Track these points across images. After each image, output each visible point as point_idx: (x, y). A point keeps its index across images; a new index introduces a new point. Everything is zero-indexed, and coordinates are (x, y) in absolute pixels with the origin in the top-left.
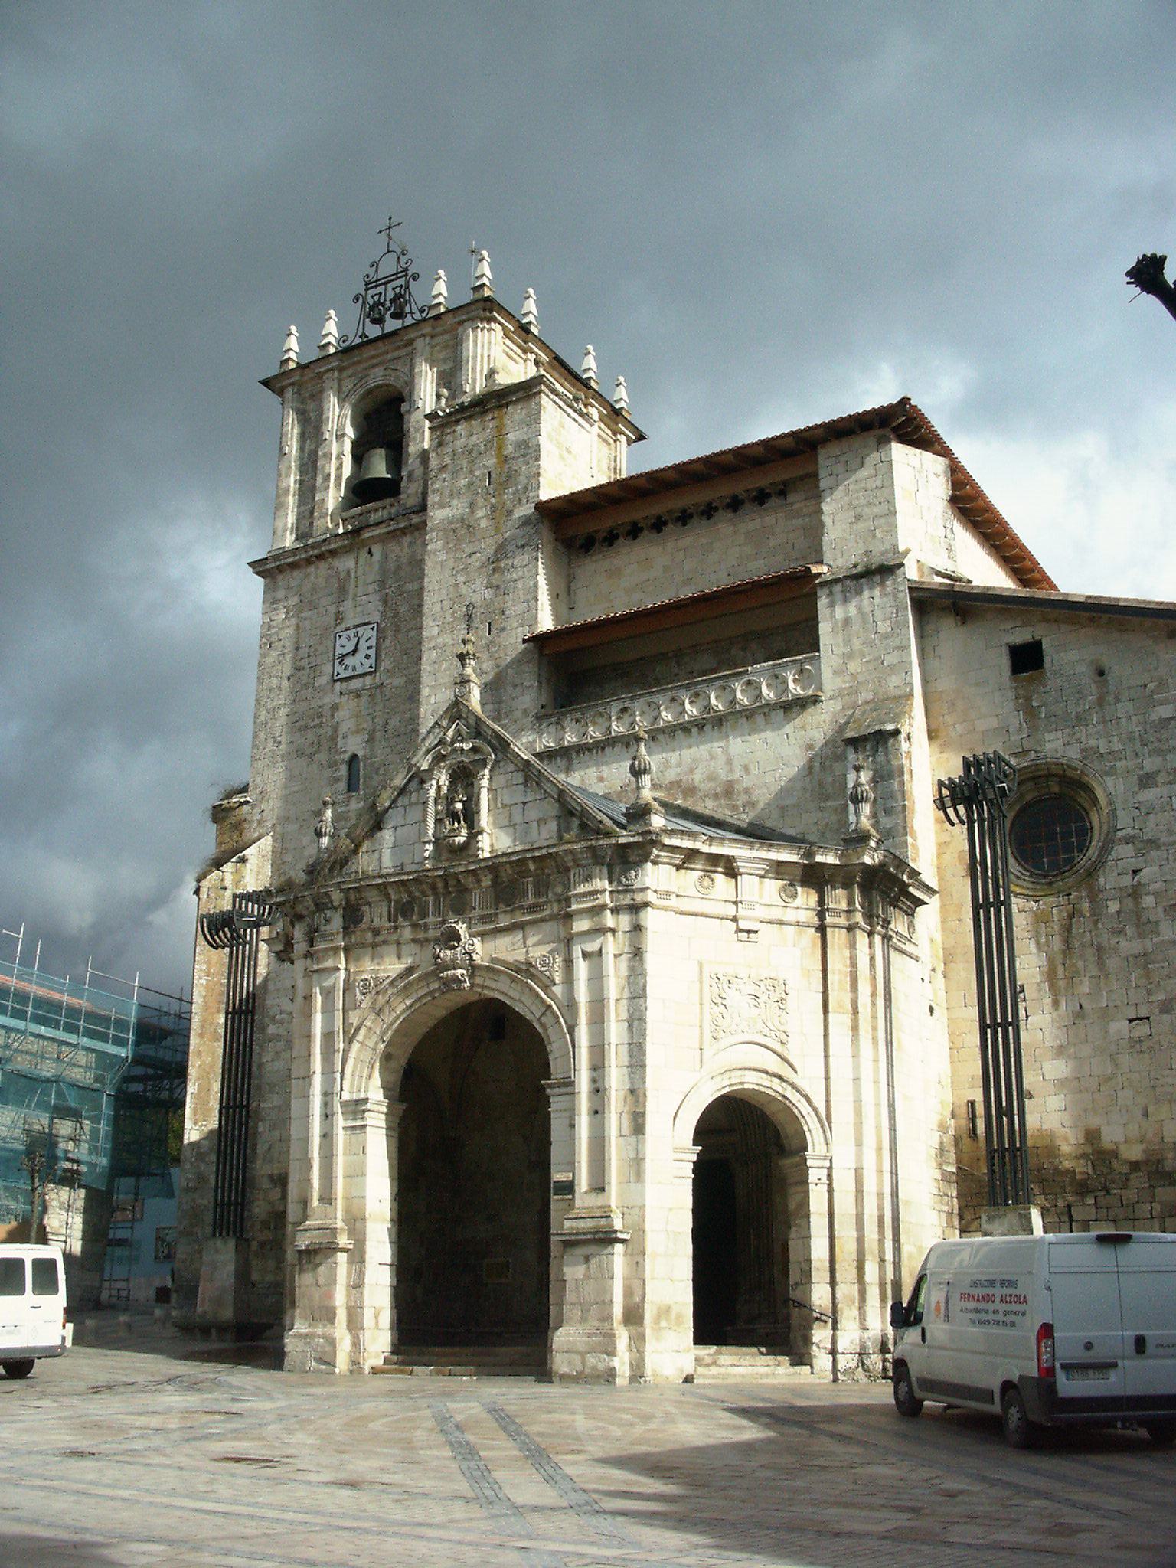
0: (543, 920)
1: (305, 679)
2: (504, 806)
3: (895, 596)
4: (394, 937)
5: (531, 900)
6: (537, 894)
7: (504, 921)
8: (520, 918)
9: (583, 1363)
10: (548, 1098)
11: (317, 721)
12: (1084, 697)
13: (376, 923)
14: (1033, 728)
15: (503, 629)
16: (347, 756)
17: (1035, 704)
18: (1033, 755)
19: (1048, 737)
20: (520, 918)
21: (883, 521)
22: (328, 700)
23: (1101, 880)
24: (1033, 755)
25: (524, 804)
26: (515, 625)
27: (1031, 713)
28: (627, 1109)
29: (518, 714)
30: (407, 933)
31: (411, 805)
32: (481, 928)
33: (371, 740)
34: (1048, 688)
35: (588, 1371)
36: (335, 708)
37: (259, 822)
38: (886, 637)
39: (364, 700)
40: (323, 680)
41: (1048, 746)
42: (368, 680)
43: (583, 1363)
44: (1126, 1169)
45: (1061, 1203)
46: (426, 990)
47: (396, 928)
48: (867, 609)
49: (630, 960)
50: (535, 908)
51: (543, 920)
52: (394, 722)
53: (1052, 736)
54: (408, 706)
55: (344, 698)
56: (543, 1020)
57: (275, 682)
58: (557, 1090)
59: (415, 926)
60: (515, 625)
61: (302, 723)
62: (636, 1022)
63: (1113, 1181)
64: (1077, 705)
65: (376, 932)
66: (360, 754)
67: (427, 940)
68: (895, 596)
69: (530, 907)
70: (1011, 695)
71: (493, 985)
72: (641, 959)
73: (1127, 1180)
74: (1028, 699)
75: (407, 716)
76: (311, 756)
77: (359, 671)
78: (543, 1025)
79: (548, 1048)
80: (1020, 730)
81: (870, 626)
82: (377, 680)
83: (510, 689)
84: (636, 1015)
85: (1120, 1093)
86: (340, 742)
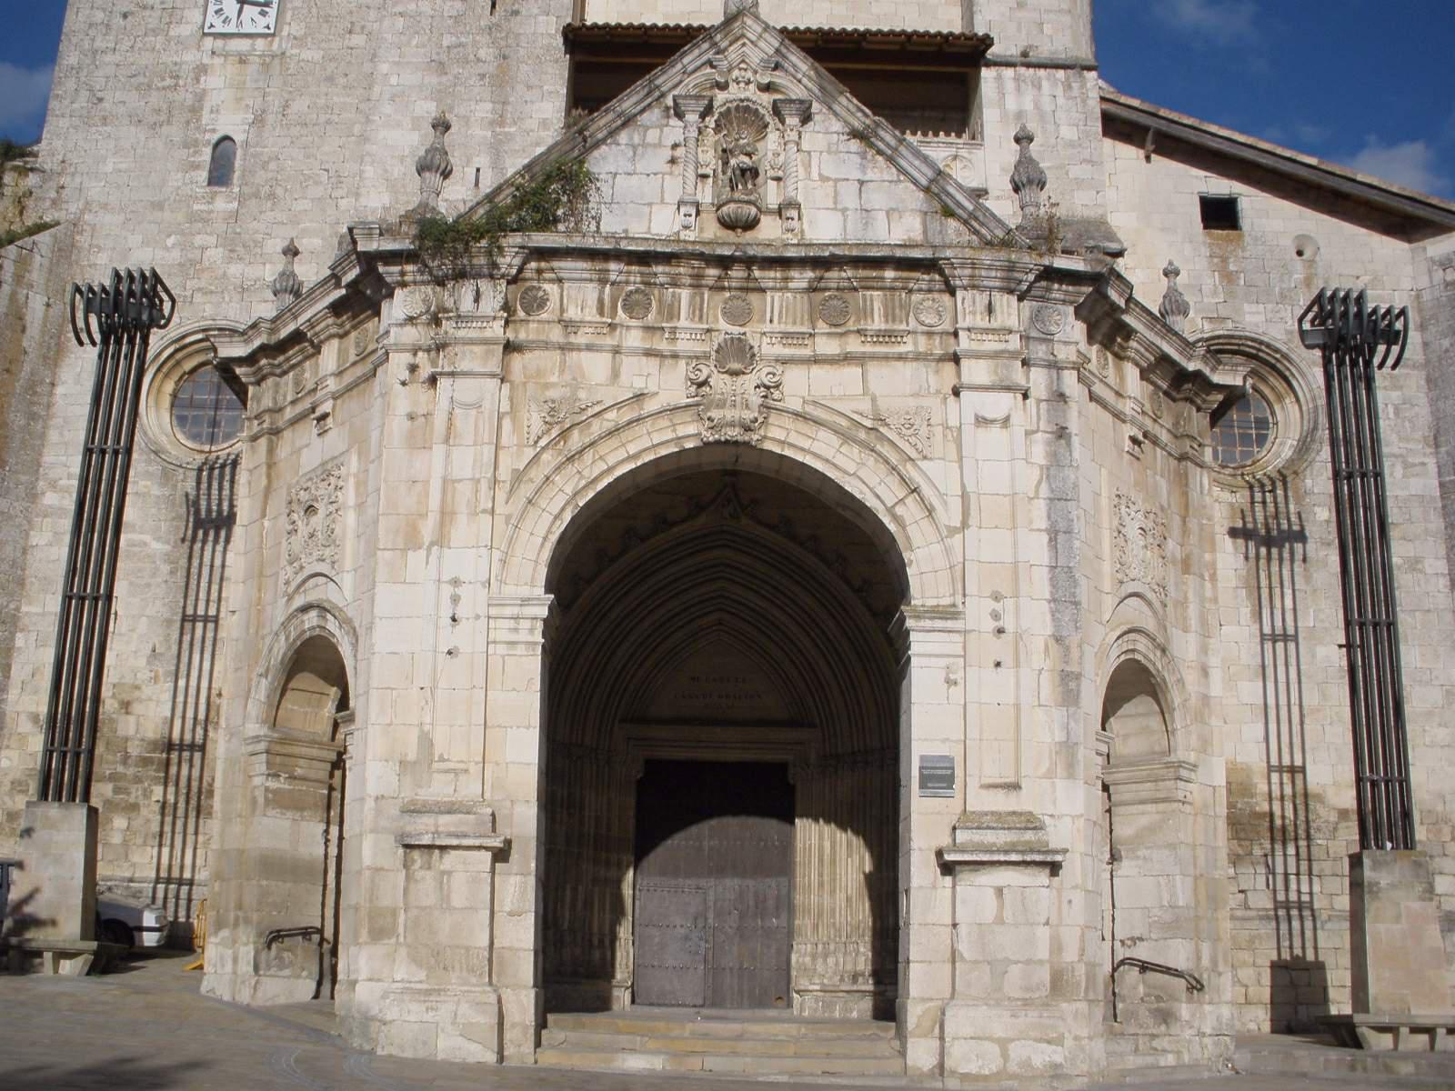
0: (901, 358)
1: (153, 23)
2: (824, 179)
3: (1084, 101)
4: (609, 341)
5: (878, 323)
6: (889, 315)
7: (828, 346)
8: (854, 345)
9: (1005, 1055)
10: (907, 633)
11: (168, 82)
12: (1290, 274)
13: (572, 313)
14: (1231, 294)
15: (516, 13)
16: (216, 137)
17: (1232, 267)
18: (1230, 325)
19: (1246, 307)
20: (854, 345)
21: (1052, 16)
22: (190, 57)
23: (1309, 482)
24: (1230, 325)
25: (861, 183)
26: (536, 11)
27: (1229, 278)
28: (1047, 665)
29: (532, 124)
30: (634, 339)
31: (644, 145)
32: (788, 352)
33: (259, 121)
34: (1247, 254)
35: (1013, 1067)
36: (201, 70)
37: (54, 202)
38: (1071, 144)
39: (253, 68)
40: (185, 31)
41: (1248, 318)
42: (260, 43)
43: (1005, 1055)
44: (1333, 817)
45: (1257, 852)
46: (669, 435)
47: (612, 327)
48: (1047, 106)
49: (1049, 443)
50: (888, 336)
51: (901, 358)
52: (299, 106)
53: (1254, 308)
54: (324, 89)
55: (218, 61)
56: (899, 510)
57: (99, 16)
58: (928, 623)
59: (649, 329)
60: (536, 11)
61: (141, 79)
62: (1061, 538)
63: (1319, 829)
64: (1281, 280)
65: (569, 326)
66: (239, 138)
67: (675, 356)
68: (1084, 101)
69: (879, 334)
70: (1205, 251)
71: (806, 444)
72: (1069, 444)
73: (1335, 829)
74: (1224, 260)
75: (322, 101)
76: (153, 126)
77: (248, 28)
78: (895, 518)
79: (906, 556)
80: (1215, 293)
81: (1051, 127)
82: (275, 46)
83: (520, 88)
84: (1062, 525)
85: (1327, 728)
86: (206, 117)
